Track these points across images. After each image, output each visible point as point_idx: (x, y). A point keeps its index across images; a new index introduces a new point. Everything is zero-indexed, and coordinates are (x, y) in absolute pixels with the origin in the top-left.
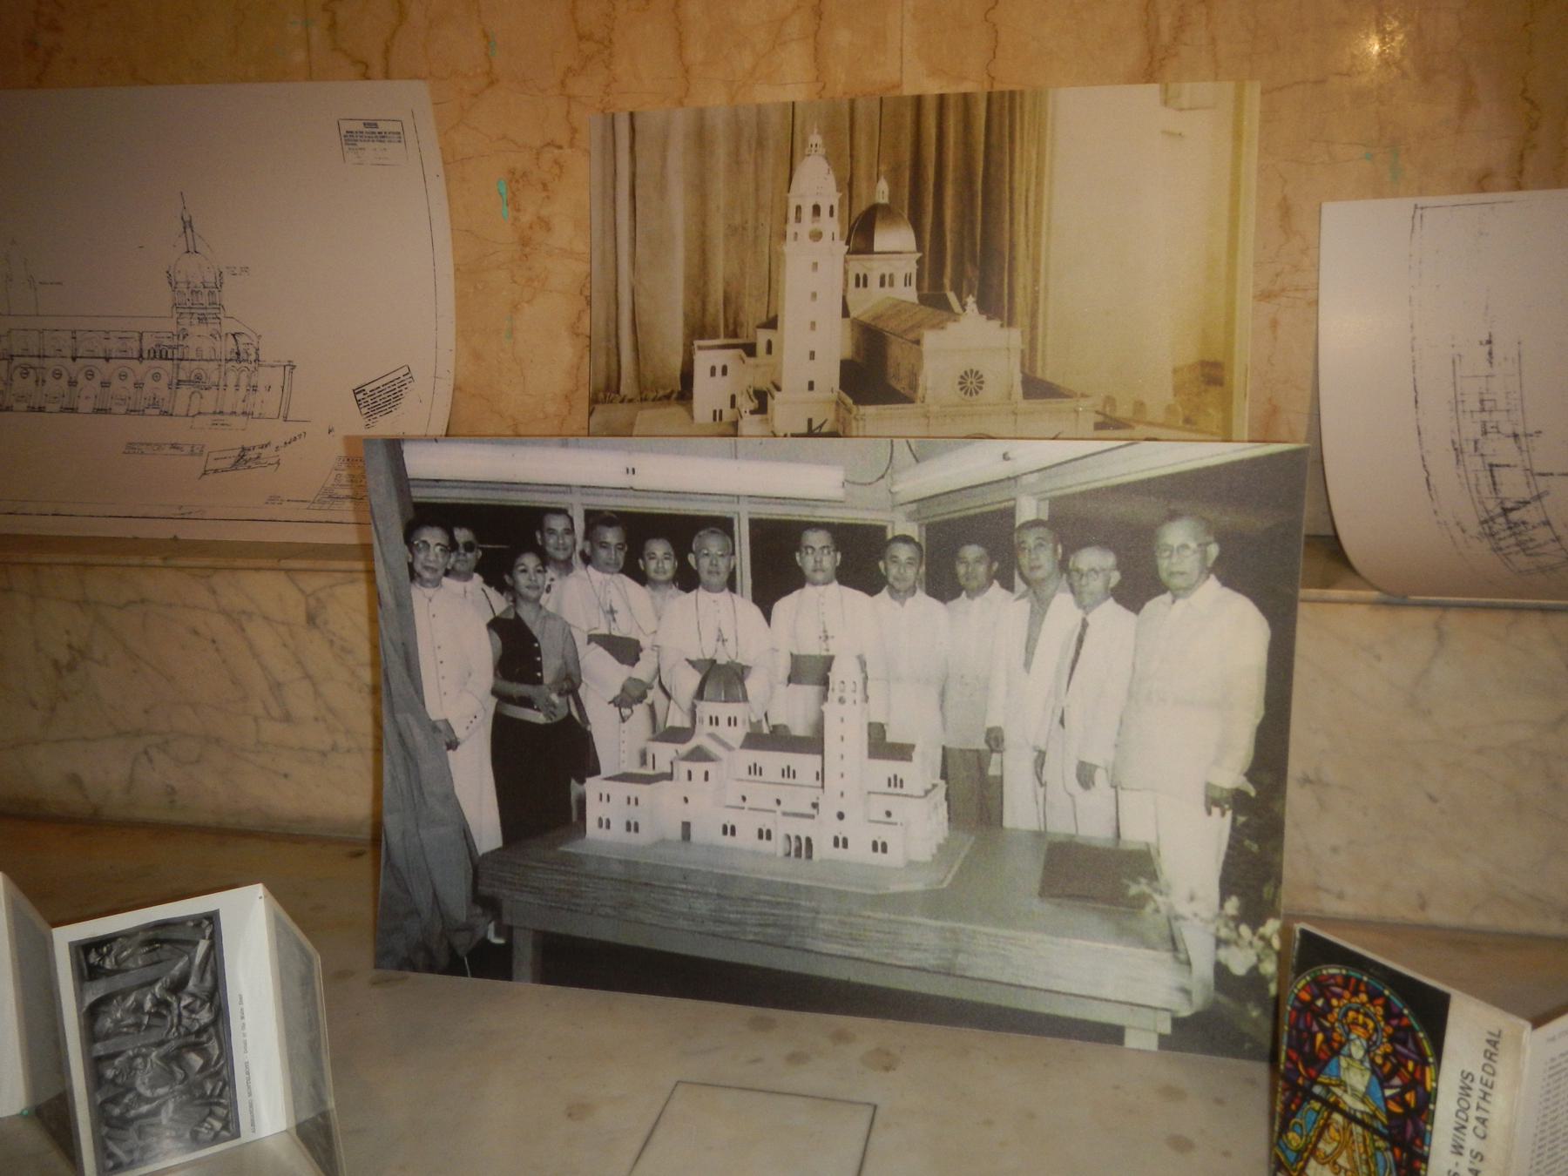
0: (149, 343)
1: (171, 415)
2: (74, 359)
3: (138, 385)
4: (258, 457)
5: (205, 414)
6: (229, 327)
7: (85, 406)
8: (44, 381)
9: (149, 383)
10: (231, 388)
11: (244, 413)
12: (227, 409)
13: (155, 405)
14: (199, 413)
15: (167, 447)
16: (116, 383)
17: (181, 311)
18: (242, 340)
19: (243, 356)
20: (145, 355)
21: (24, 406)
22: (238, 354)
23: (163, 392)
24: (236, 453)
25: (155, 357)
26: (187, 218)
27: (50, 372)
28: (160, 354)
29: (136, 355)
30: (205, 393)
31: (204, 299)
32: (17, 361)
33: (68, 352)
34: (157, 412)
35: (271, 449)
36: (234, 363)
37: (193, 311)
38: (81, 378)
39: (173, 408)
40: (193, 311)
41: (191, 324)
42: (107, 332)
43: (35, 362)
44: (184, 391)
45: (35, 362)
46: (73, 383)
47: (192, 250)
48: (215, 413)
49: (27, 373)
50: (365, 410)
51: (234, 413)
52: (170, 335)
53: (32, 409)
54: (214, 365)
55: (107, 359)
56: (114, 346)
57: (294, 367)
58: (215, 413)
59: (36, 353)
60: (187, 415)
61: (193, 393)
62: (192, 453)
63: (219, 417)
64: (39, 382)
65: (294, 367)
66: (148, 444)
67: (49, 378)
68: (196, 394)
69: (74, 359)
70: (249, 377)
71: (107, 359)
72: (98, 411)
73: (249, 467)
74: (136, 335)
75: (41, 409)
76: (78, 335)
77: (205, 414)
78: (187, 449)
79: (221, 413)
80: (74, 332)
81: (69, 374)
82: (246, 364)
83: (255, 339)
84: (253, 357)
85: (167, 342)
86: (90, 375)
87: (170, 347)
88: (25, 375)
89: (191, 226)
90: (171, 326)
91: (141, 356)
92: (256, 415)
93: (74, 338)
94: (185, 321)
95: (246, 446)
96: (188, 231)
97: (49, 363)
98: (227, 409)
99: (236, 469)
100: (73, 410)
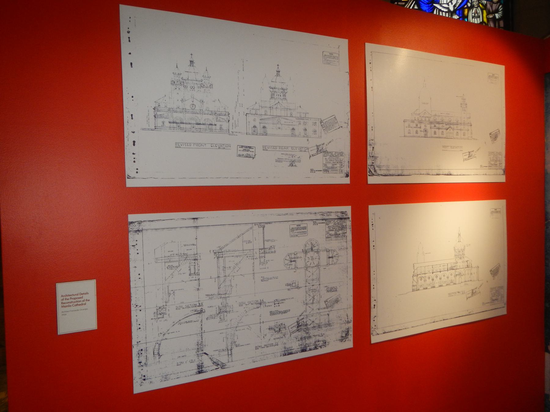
0: (449, 266)
1: (456, 284)
2: (433, 273)
3: (448, 277)
4: (476, 292)
5: (463, 282)
6: (466, 259)
7: (437, 285)
8: (426, 280)
9: (450, 276)
10: (467, 275)
11: (470, 281)
12: (467, 281)
13: (452, 282)
14: (461, 282)
15: (457, 293)
16: (443, 278)
17: (456, 257)
18: (468, 262)
19: (469, 266)
20: (449, 269)
21: (422, 288)
22: (468, 266)
23: (453, 278)
24: (471, 292)
25: (451, 269)
26: (459, 233)
27: (427, 278)
28: (452, 269)
29: (447, 270)
30: (462, 277)
31: (461, 253)
32: (419, 276)
33: (431, 272)
34: (452, 284)
35: (478, 288)
36: (467, 268)
37: (459, 256)
38: (435, 279)
39: (456, 282)
40: (459, 256)
41: (458, 260)
42: (440, 265)
43: (423, 275)
44: (458, 277)
45: (423, 275)
46: (433, 280)
47: (459, 241)
48: (465, 282)
49: (422, 279)
50: (493, 275)
51: (468, 281)
52: (453, 263)
53: (424, 289)
54: (463, 269)
55: (440, 272)
56: (442, 268)
57: (478, 267)
58: (465, 282)
59: (423, 273)
60: (459, 283)
61: (459, 277)
62: (463, 294)
63: (466, 282)
64: (425, 281)
65: (478, 267)
66: (453, 293)
67: (427, 279)
68: (460, 278)
69: (433, 273)
70: (470, 271)
71: (440, 272)
72: (440, 286)
73: (475, 295)
74: (447, 265)
75: (426, 288)
76: (434, 266)
77: (463, 282)
78: (461, 292)
79: (466, 281)
80: (433, 266)
81: (432, 277)
82: (469, 268)
83: (471, 262)
84: (471, 266)
85: (453, 265)
86: (437, 277)
87: (454, 266)
88: (421, 280)
89: (460, 235)
90: (454, 261)
91: (448, 270)
92: (473, 280)
93: (433, 267)
94: (457, 259)
95: (473, 289)
96: (459, 236)
97: (427, 275)
98: (467, 281)
99: (473, 296)
100: (434, 287)
